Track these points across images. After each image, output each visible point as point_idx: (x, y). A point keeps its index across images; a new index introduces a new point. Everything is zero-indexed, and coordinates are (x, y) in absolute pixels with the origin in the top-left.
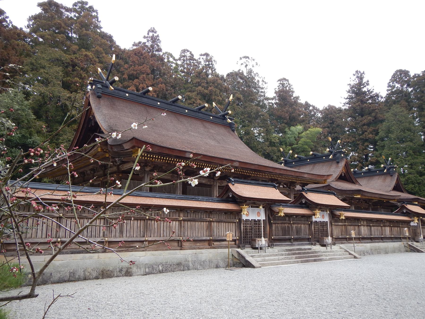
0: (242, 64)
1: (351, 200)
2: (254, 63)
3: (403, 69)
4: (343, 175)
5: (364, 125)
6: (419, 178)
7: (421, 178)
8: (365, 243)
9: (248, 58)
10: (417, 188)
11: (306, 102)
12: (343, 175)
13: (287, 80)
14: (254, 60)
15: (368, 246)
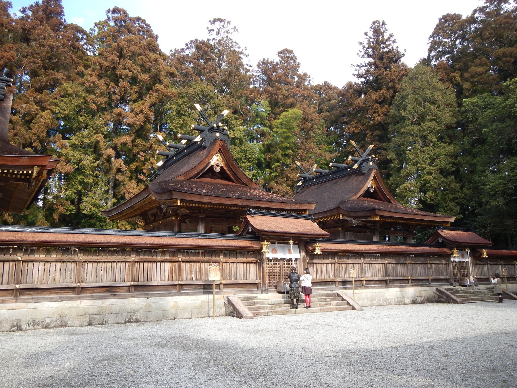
0: (213, 30)
1: (200, 213)
2: (229, 27)
3: (452, 13)
4: (218, 170)
5: (376, 102)
6: (443, 179)
7: (445, 180)
8: (36, 301)
9: (220, 20)
10: (439, 198)
11: (326, 83)
12: (218, 170)
13: (291, 52)
14: (229, 23)
15: (49, 308)
